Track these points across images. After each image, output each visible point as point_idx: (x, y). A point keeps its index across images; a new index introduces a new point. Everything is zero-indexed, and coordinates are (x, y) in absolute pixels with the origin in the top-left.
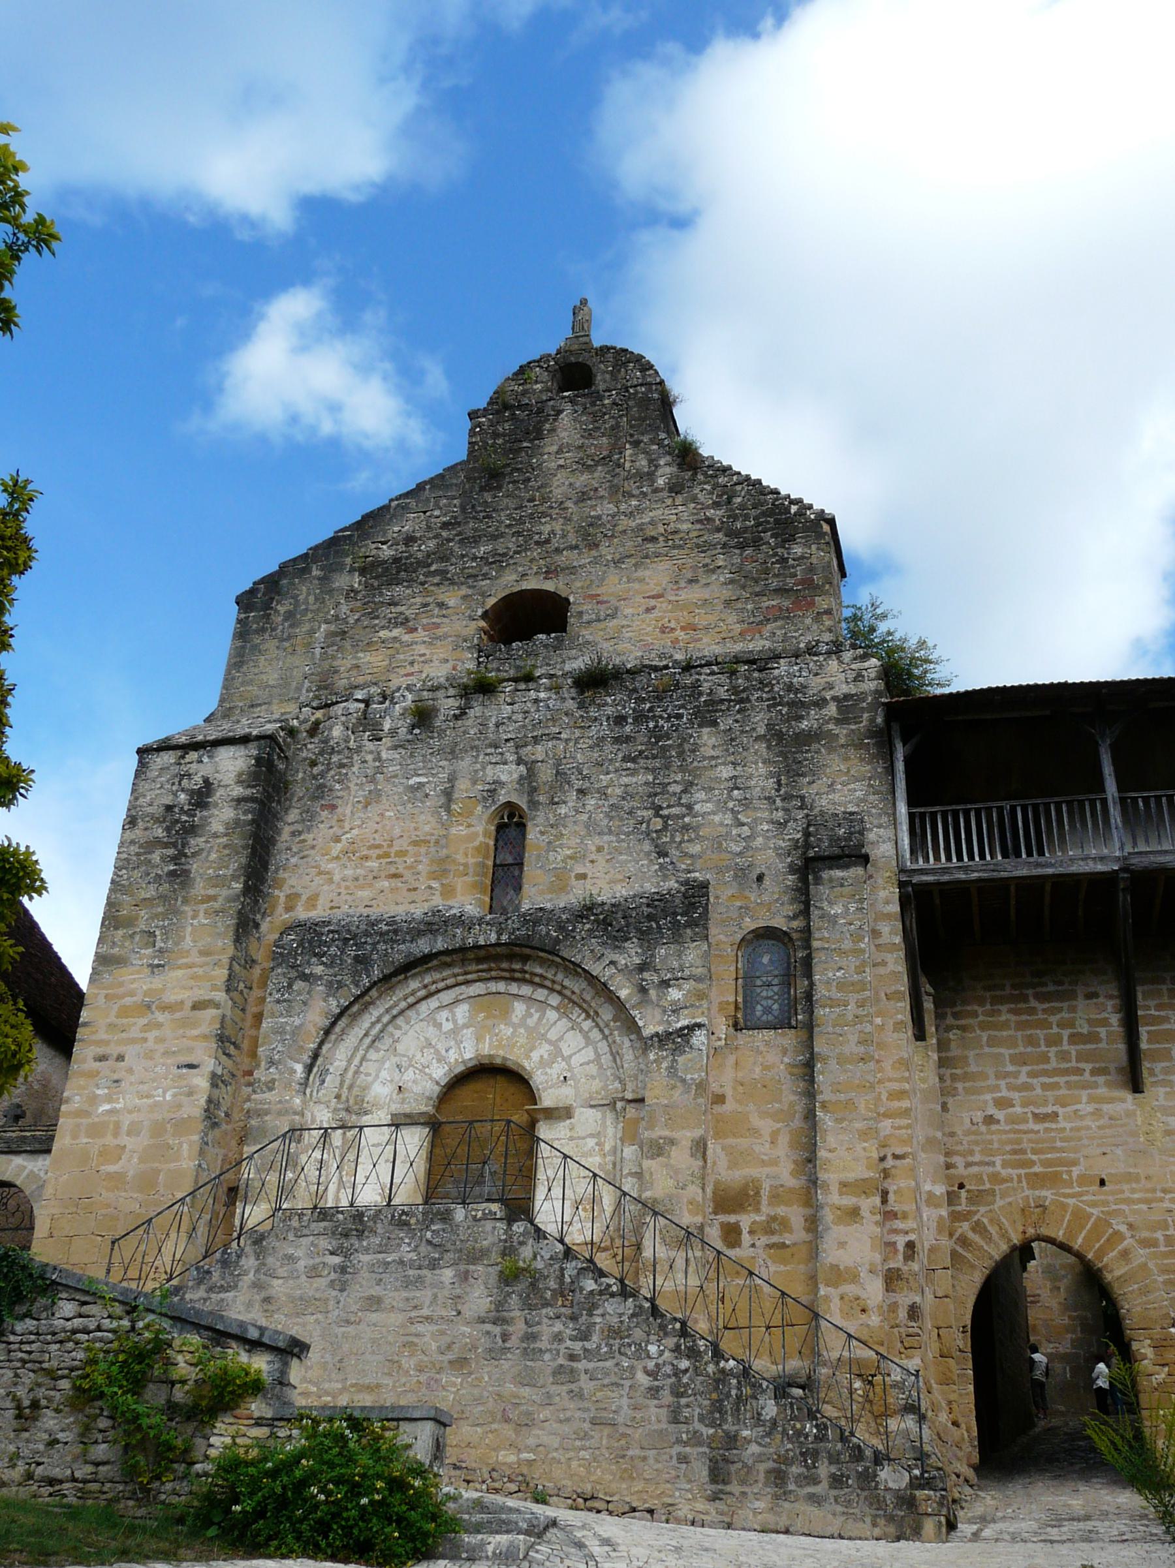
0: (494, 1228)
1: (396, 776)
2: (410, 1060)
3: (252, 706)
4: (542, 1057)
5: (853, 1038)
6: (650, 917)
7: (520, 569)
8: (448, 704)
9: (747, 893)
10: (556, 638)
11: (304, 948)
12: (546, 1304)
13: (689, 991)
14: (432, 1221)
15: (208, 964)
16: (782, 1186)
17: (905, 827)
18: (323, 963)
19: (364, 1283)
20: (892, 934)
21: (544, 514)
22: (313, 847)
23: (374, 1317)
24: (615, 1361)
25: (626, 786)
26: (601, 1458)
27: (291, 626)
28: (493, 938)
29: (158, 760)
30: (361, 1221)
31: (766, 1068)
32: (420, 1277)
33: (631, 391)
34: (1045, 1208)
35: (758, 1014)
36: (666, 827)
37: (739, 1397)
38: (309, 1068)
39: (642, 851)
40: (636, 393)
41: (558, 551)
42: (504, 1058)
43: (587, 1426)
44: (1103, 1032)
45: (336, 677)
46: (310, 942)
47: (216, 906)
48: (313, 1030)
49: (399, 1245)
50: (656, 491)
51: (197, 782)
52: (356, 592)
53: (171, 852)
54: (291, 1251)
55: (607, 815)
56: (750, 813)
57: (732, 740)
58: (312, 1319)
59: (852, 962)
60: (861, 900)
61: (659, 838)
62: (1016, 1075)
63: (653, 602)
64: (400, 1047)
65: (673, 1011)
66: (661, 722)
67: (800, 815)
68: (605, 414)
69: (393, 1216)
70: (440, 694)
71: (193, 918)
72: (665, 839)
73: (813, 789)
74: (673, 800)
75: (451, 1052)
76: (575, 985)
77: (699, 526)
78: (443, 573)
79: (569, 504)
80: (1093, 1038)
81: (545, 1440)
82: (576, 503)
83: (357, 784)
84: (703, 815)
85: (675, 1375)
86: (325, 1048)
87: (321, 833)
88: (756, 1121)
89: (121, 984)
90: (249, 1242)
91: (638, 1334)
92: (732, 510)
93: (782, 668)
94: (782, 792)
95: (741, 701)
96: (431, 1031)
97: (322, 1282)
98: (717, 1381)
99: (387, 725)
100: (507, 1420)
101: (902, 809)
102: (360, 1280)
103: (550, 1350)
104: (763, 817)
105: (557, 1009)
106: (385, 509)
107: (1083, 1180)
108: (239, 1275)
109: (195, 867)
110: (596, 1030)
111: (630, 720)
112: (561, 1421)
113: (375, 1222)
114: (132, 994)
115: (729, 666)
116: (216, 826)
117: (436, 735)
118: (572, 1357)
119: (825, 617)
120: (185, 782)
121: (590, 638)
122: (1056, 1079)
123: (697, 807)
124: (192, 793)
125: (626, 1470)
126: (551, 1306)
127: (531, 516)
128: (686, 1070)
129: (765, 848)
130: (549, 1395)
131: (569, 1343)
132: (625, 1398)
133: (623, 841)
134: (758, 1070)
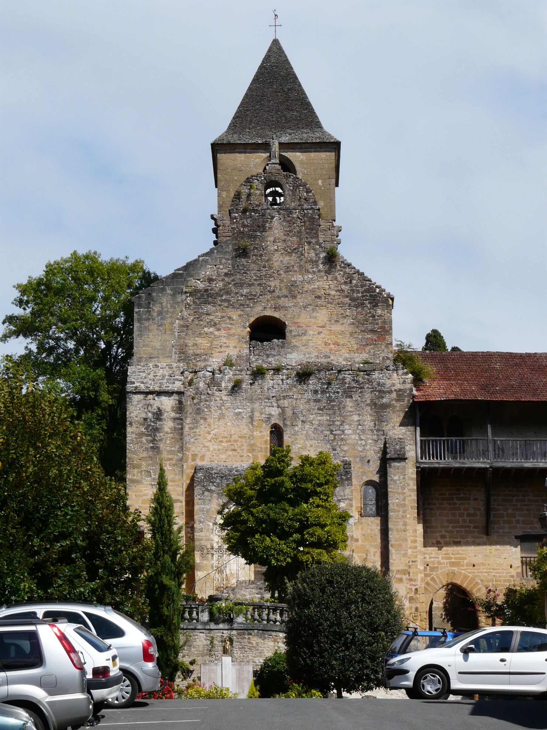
1: (230, 408)
3: (150, 358)
5: (401, 523)
7: (263, 304)
8: (247, 378)
10: (282, 342)
17: (419, 445)
18: (215, 486)
20: (413, 485)
21: (271, 276)
22: (200, 435)
25: (320, 420)
27: (161, 319)
31: (371, 530)
33: (305, 211)
34: (455, 573)
35: (368, 510)
36: (335, 438)
40: (308, 213)
41: (279, 297)
44: (478, 513)
45: (187, 348)
46: (209, 477)
47: (174, 462)
50: (319, 271)
51: (154, 409)
52: (190, 305)
53: (150, 438)
54: (244, 593)
55: (313, 432)
56: (365, 435)
57: (358, 405)
59: (401, 497)
60: (405, 475)
61: (333, 443)
62: (448, 527)
63: (321, 330)
66: (331, 395)
67: (383, 438)
68: (294, 223)
72: (335, 444)
74: (337, 428)
77: (338, 293)
78: (228, 301)
79: (281, 272)
80: (475, 515)
82: (285, 272)
84: (348, 435)
87: (202, 428)
89: (141, 491)
92: (352, 287)
93: (376, 375)
95: (361, 388)
99: (223, 385)
101: (418, 438)
104: (369, 438)
106: (196, 261)
107: (468, 565)
111: (319, 392)
114: (145, 495)
120: (150, 408)
121: (296, 344)
122: (461, 529)
123: (346, 431)
124: (153, 414)
127: (265, 276)
129: (370, 449)
133: (320, 443)
134: (369, 531)
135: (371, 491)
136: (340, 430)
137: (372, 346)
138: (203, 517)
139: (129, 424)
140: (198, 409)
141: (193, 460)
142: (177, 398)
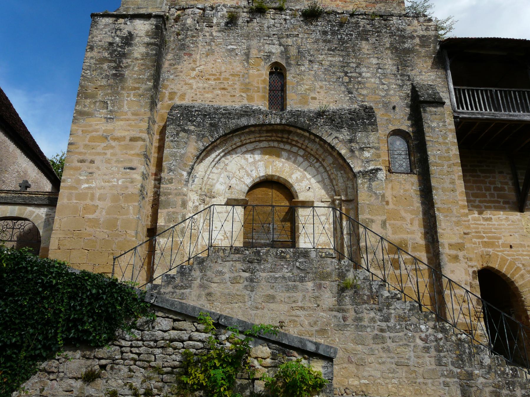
0: (332, 262)
1: (221, 44)
2: (234, 174)
3: (139, 8)
4: (297, 178)
5: (448, 181)
6: (351, 119)
8: (244, 16)
9: (389, 114)
11: (183, 117)
12: (365, 303)
13: (373, 154)
14: (299, 257)
15: (137, 120)
16: (417, 243)
17: (453, 93)
18: (194, 125)
19: (264, 287)
20: (452, 138)
22: (181, 72)
23: (272, 306)
24: (404, 333)
25: (331, 61)
26: (403, 383)
28: (278, 121)
29: (103, 20)
30: (259, 255)
31: (405, 191)
32: (295, 286)
35: (397, 167)
36: (350, 81)
37: (470, 353)
38: (189, 174)
39: (341, 90)
42: (279, 177)
43: (394, 366)
44: (506, 187)
47: (140, 92)
48: (191, 156)
49: (282, 269)
53: (113, 64)
55: (323, 73)
56: (387, 80)
57: (376, 48)
58: (236, 305)
59: (444, 148)
62: (474, 201)
64: (228, 168)
65: (367, 162)
67: (409, 83)
69: (277, 253)
70: (240, 10)
71: (128, 97)
72: (350, 86)
73: (413, 73)
74: (352, 70)
75: (254, 172)
76: (313, 147)
80: (502, 189)
81: (373, 373)
83: (202, 46)
84: (367, 78)
85: (436, 341)
86: (196, 165)
87: (185, 65)
88: (403, 214)
89: (91, 126)
90: (195, 263)
91: (414, 319)
93: (394, 20)
94: (400, 72)
95: (378, 32)
96: (243, 162)
97: (240, 286)
98: (458, 345)
99: (215, 21)
100: (351, 362)
101: (452, 86)
102: (262, 286)
103: (370, 326)
104: (393, 83)
105: (303, 156)
107: (503, 245)
108: (191, 280)
109: (127, 73)
110: (321, 168)
111: (329, 33)
112: (380, 363)
113: (267, 256)
114: (96, 131)
115: (371, 17)
116: (136, 55)
117: (239, 28)
118: (382, 330)
119: (402, 4)
122: (489, 204)
123: (364, 74)
124: (122, 38)
125: (417, 390)
126: (367, 303)
128: (376, 189)
130: (372, 350)
131: (379, 323)
132: (412, 352)
133: (331, 85)
135: (400, 144)
136: (356, 72)
137: (383, 4)
138: (174, 163)
139: (90, 48)
140: (183, 45)
141: (171, 99)
142: (155, 23)
